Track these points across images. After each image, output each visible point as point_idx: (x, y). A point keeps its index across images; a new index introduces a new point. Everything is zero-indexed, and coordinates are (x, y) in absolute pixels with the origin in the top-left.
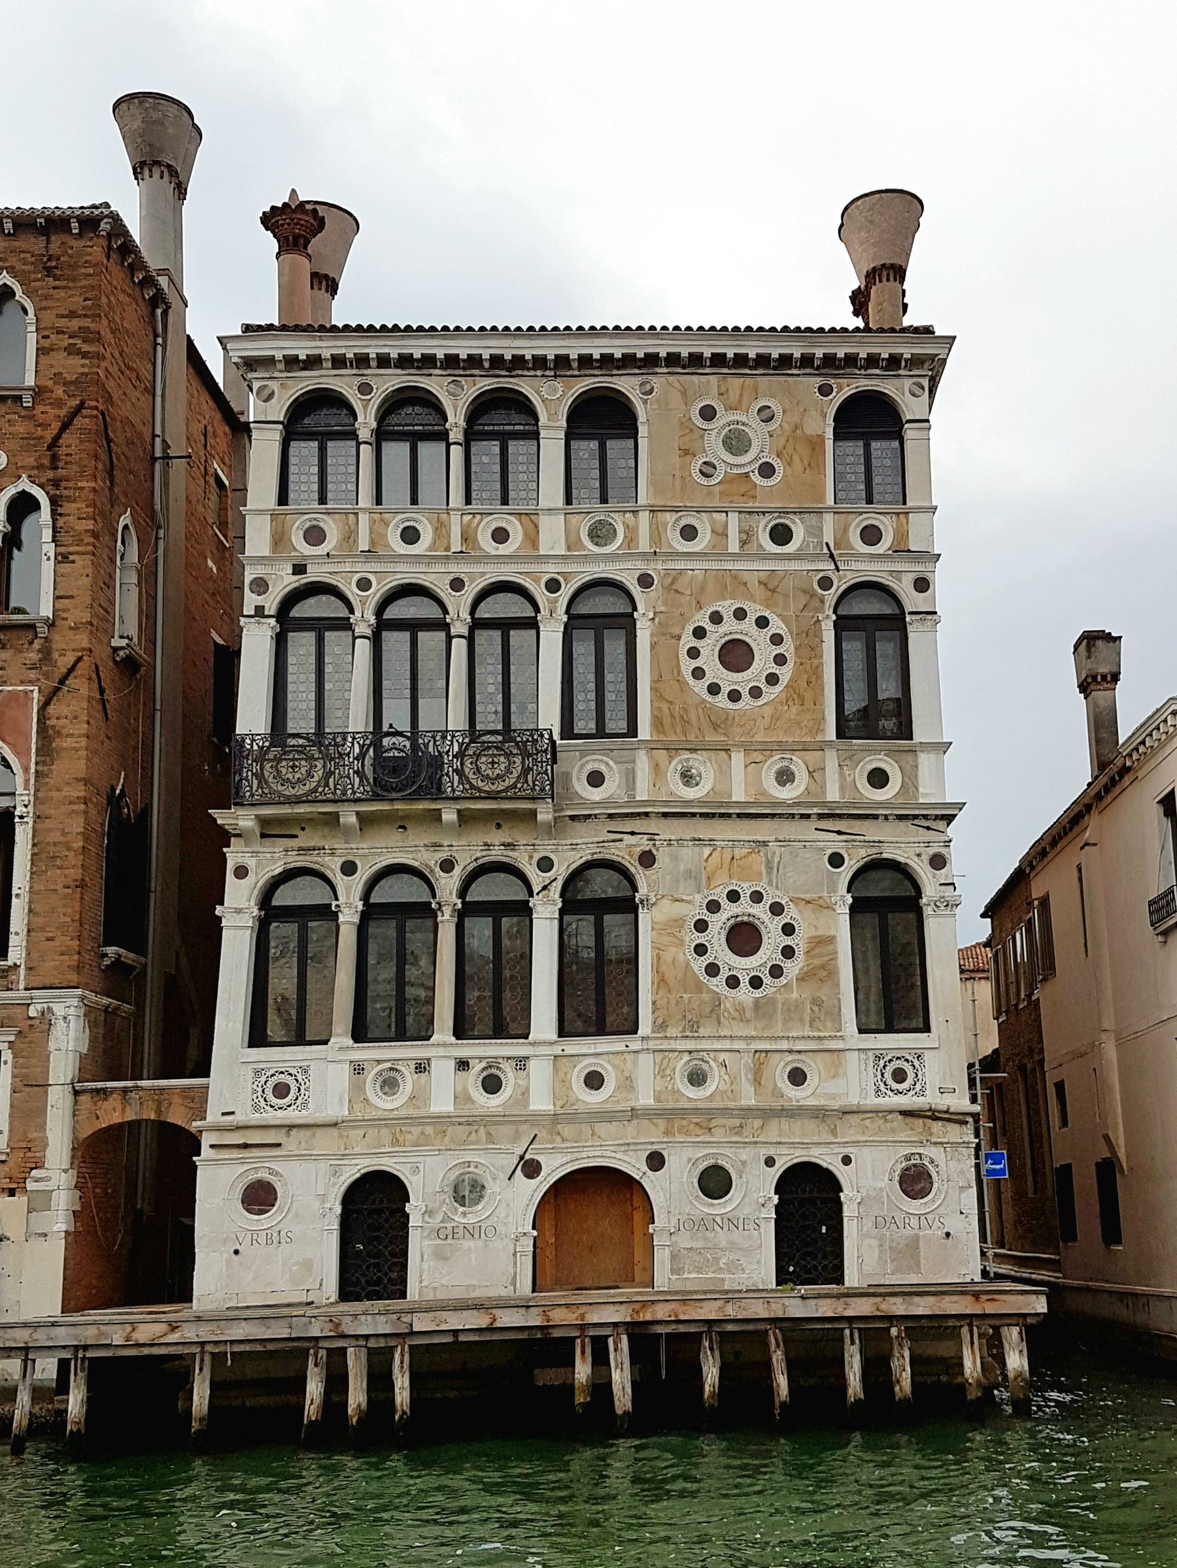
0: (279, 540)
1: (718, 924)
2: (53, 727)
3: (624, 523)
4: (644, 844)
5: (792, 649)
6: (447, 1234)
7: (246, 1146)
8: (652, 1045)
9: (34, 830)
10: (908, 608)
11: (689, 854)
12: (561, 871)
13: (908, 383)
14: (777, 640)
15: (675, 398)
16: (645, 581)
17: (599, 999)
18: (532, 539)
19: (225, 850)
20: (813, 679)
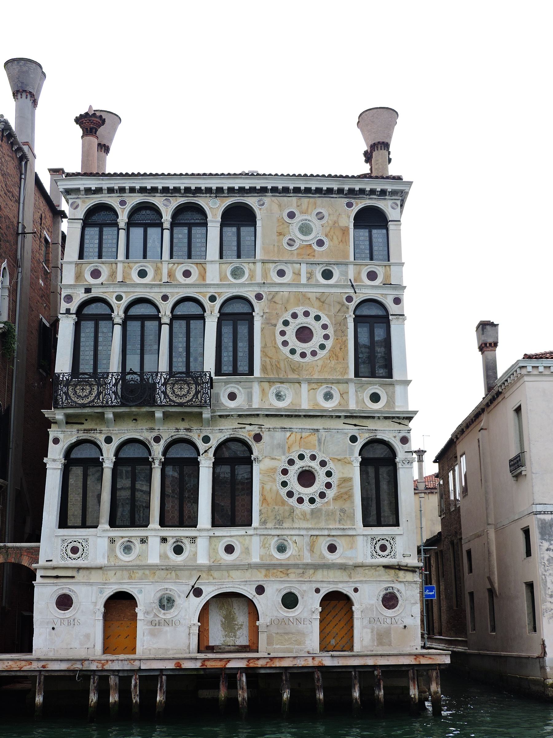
0: (79, 276)
1: (294, 471)
3: (249, 268)
4: (256, 430)
5: (333, 332)
6: (155, 624)
7: (57, 577)
8: (259, 532)
10: (391, 312)
11: (279, 436)
12: (214, 443)
13: (390, 203)
14: (325, 327)
15: (275, 208)
16: (259, 297)
17: (233, 509)
18: (203, 276)
19: (48, 430)
20: (343, 347)
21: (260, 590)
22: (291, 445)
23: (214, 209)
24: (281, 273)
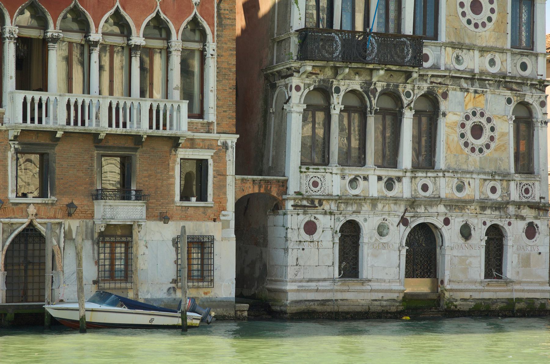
9: (217, 62)
21: (447, 222)
22: (468, 104)
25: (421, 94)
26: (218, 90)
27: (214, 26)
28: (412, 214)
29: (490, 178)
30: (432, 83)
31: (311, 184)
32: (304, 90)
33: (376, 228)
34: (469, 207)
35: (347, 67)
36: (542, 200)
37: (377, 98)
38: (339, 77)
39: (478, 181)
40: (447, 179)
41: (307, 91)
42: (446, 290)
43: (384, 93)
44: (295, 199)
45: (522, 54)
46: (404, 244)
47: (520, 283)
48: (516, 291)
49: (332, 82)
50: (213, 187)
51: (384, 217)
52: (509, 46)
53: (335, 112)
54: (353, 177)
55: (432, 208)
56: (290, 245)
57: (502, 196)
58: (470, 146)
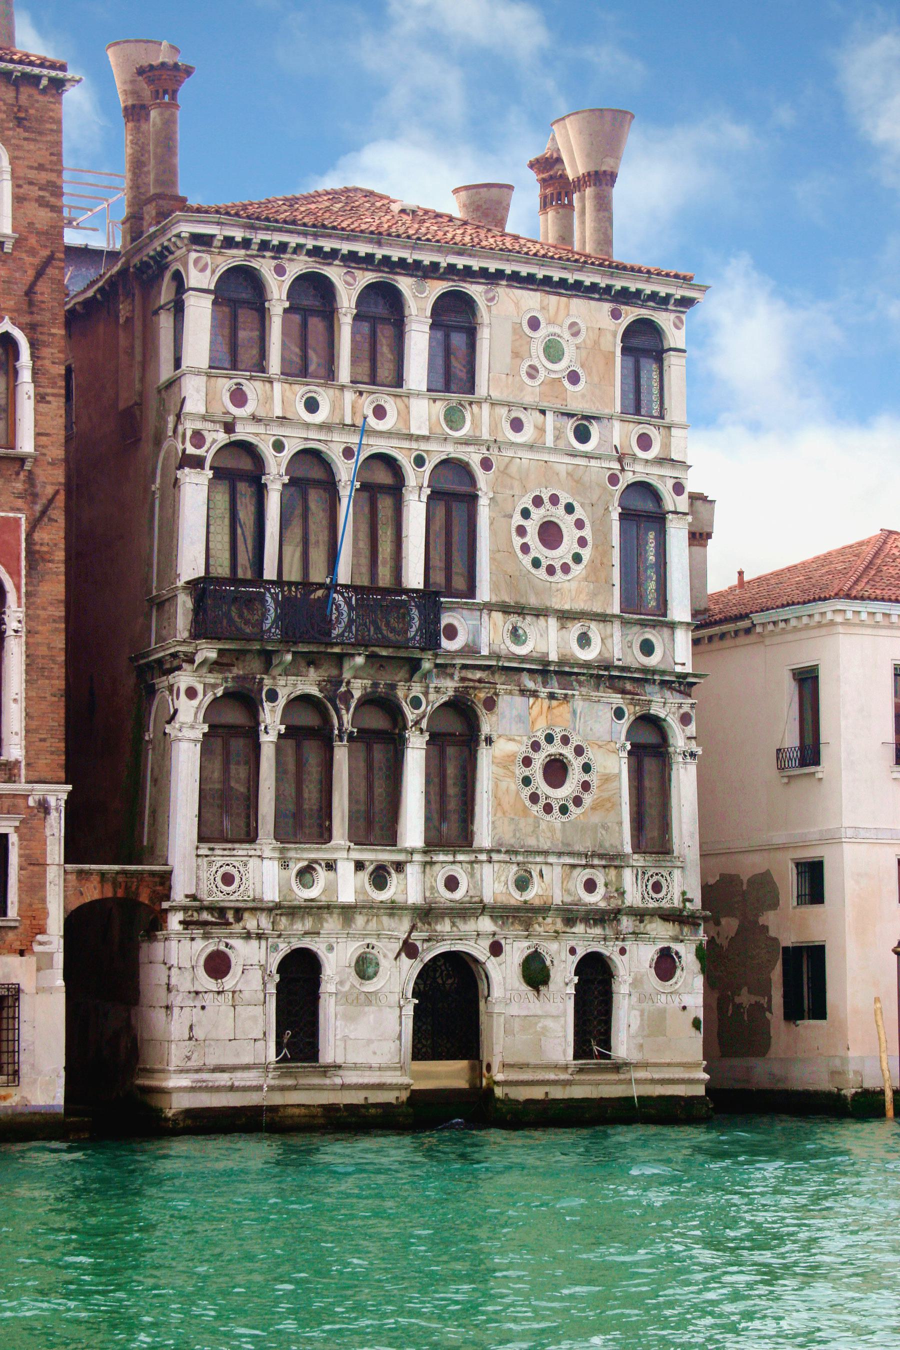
2: (39, 552)
9: (27, 644)
13: (672, 316)
16: (486, 464)
21: (496, 949)
22: (536, 719)
23: (419, 300)
24: (517, 425)
25: (442, 701)
26: (27, 698)
27: (19, 575)
28: (425, 935)
29: (584, 862)
30: (463, 679)
31: (219, 879)
32: (205, 695)
33: (353, 964)
34: (541, 919)
35: (288, 651)
36: (688, 904)
37: (352, 710)
38: (276, 671)
39: (558, 869)
40: (497, 866)
41: (209, 697)
42: (497, 1083)
43: (367, 701)
44: (185, 909)
45: (643, 624)
46: (410, 995)
47: (646, 1065)
48: (639, 1082)
49: (262, 679)
50: (20, 889)
51: (368, 941)
52: (616, 610)
53: (268, 740)
54: (306, 863)
55: (465, 923)
56: (177, 1000)
57: (607, 898)
58: (542, 802)
